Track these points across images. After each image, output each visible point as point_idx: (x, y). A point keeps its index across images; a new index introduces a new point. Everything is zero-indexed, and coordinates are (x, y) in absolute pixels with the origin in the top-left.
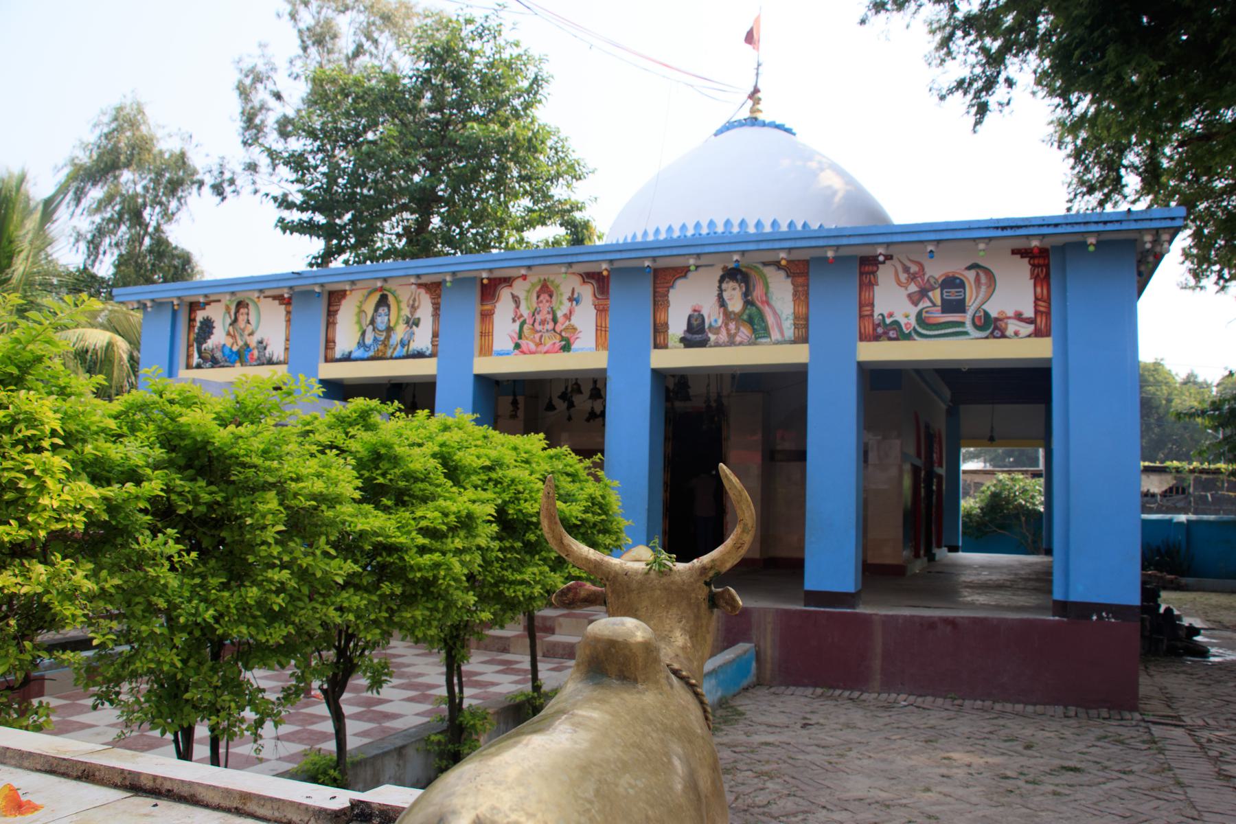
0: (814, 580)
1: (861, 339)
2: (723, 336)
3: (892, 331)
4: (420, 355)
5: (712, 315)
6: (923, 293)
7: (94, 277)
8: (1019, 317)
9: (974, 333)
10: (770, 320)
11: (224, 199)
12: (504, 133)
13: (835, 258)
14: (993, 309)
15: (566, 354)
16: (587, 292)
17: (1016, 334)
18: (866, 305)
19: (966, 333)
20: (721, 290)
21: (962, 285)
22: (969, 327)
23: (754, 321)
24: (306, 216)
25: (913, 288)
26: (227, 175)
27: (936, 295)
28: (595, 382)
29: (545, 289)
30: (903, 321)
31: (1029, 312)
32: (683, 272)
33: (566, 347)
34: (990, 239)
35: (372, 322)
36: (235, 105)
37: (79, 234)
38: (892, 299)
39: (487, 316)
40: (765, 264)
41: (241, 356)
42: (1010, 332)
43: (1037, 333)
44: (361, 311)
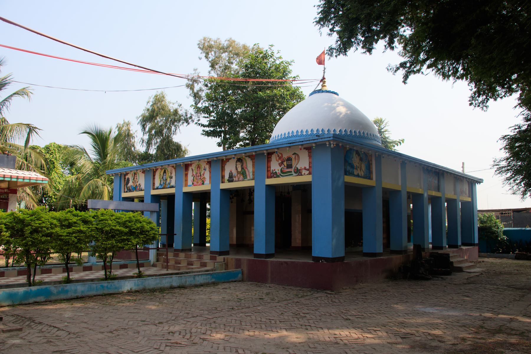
0: (256, 251)
1: (268, 178)
2: (237, 179)
3: (274, 175)
4: (172, 187)
5: (234, 173)
6: (282, 163)
7: (150, 154)
8: (305, 169)
9: (295, 174)
10: (247, 173)
11: (188, 124)
12: (271, 94)
13: (256, 155)
14: (299, 167)
15: (203, 186)
16: (207, 167)
17: (304, 174)
18: (269, 167)
19: (292, 174)
20: (236, 165)
21: (291, 160)
22: (293, 173)
23: (243, 174)
24: (212, 129)
25: (280, 161)
26: (189, 116)
27: (285, 163)
28: (250, 189)
29: (199, 167)
30: (277, 172)
31: (308, 167)
32: (228, 160)
33: (203, 184)
34: (290, 147)
35: (163, 178)
36: (188, 91)
37: (143, 141)
38: (275, 166)
39: (186, 175)
40: (246, 156)
41: (135, 189)
42: (303, 174)
43: (310, 174)
44: (160, 175)
